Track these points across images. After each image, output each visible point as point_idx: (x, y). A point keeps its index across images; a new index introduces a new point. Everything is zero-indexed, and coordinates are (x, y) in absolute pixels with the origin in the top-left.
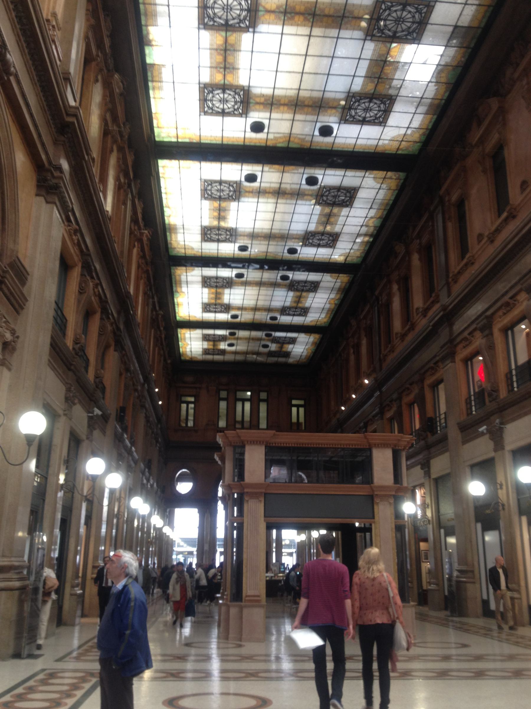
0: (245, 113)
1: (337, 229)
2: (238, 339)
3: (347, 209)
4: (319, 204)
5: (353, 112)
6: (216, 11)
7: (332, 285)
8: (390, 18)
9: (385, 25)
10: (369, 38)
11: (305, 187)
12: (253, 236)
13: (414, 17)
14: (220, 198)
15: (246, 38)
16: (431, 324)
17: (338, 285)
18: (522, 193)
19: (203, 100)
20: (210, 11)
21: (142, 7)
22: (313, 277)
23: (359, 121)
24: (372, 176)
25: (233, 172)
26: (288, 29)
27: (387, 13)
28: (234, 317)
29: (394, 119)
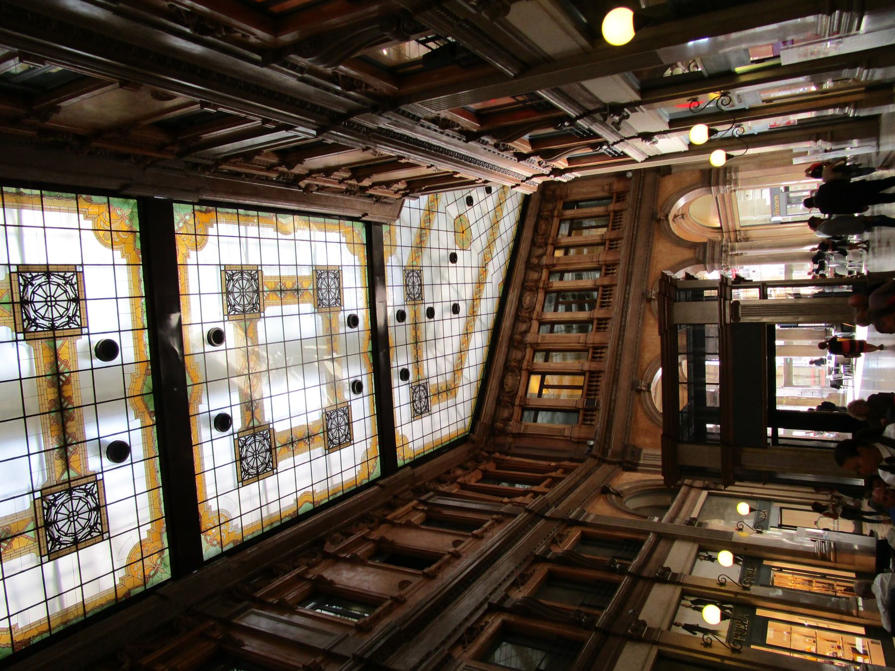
6: (259, 463)
10: (262, 314)
11: (408, 320)
15: (279, 428)
19: (340, 446)
25: (401, 394)
27: (237, 307)
29: (334, 261)
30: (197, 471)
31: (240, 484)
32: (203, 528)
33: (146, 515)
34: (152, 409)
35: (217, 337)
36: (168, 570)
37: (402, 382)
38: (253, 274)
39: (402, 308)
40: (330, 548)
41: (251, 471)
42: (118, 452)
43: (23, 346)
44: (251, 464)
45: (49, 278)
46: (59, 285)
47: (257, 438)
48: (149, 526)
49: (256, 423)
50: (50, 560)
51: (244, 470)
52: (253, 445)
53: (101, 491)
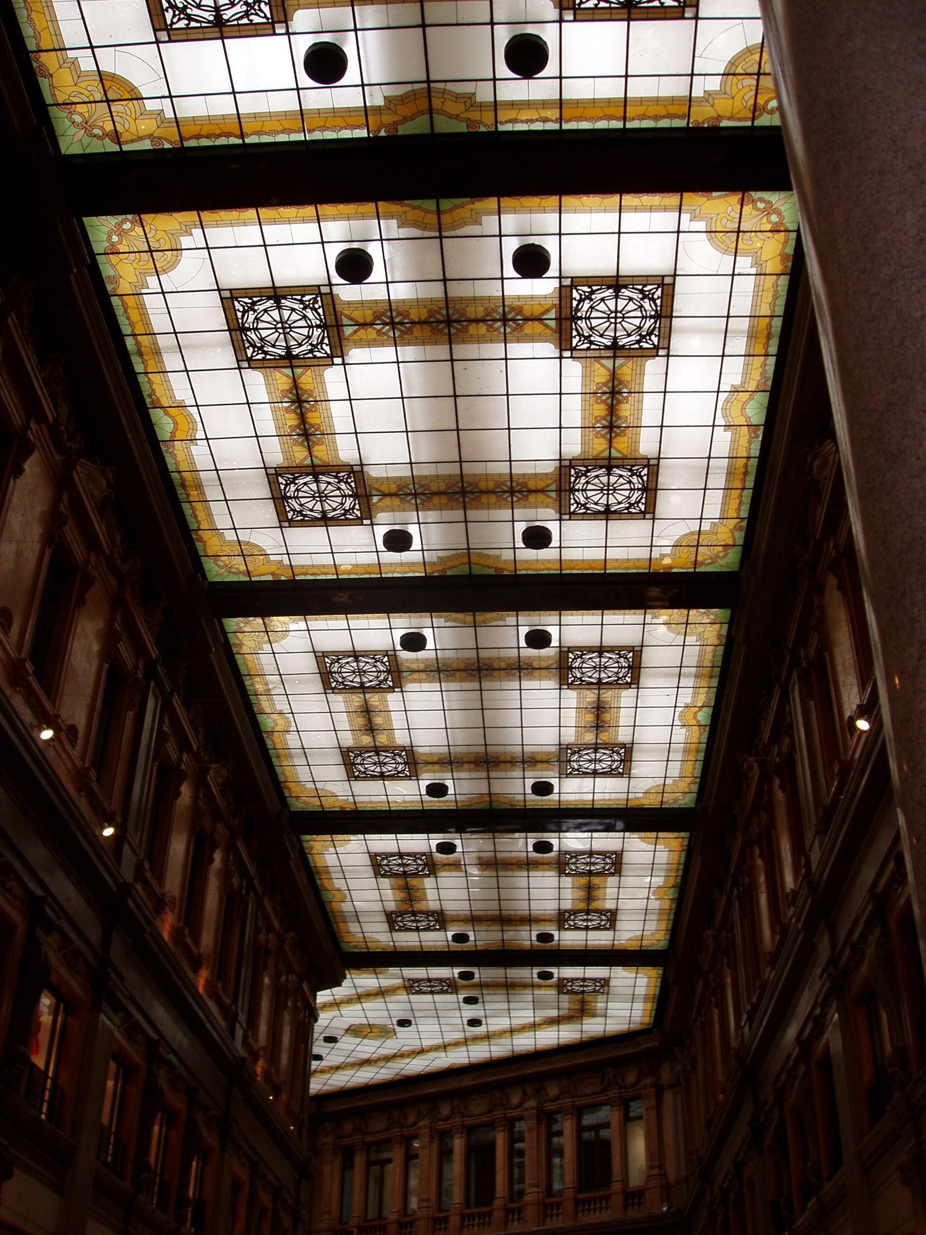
0: (366, 516)
2: (481, 986)
6: (264, 333)
8: (594, 314)
12: (450, 762)
14: (363, 688)
15: (333, 377)
19: (279, 499)
20: (252, 335)
21: (130, 343)
23: (599, 512)
28: (460, 938)
30: (263, 211)
31: (227, 294)
32: (147, 218)
33: (191, 109)
35: (531, 261)
36: (76, 150)
37: (398, 634)
39: (555, 643)
40: (81, 473)
41: (251, 316)
44: (266, 317)
47: (317, 332)
48: (169, 114)
49: (348, 331)
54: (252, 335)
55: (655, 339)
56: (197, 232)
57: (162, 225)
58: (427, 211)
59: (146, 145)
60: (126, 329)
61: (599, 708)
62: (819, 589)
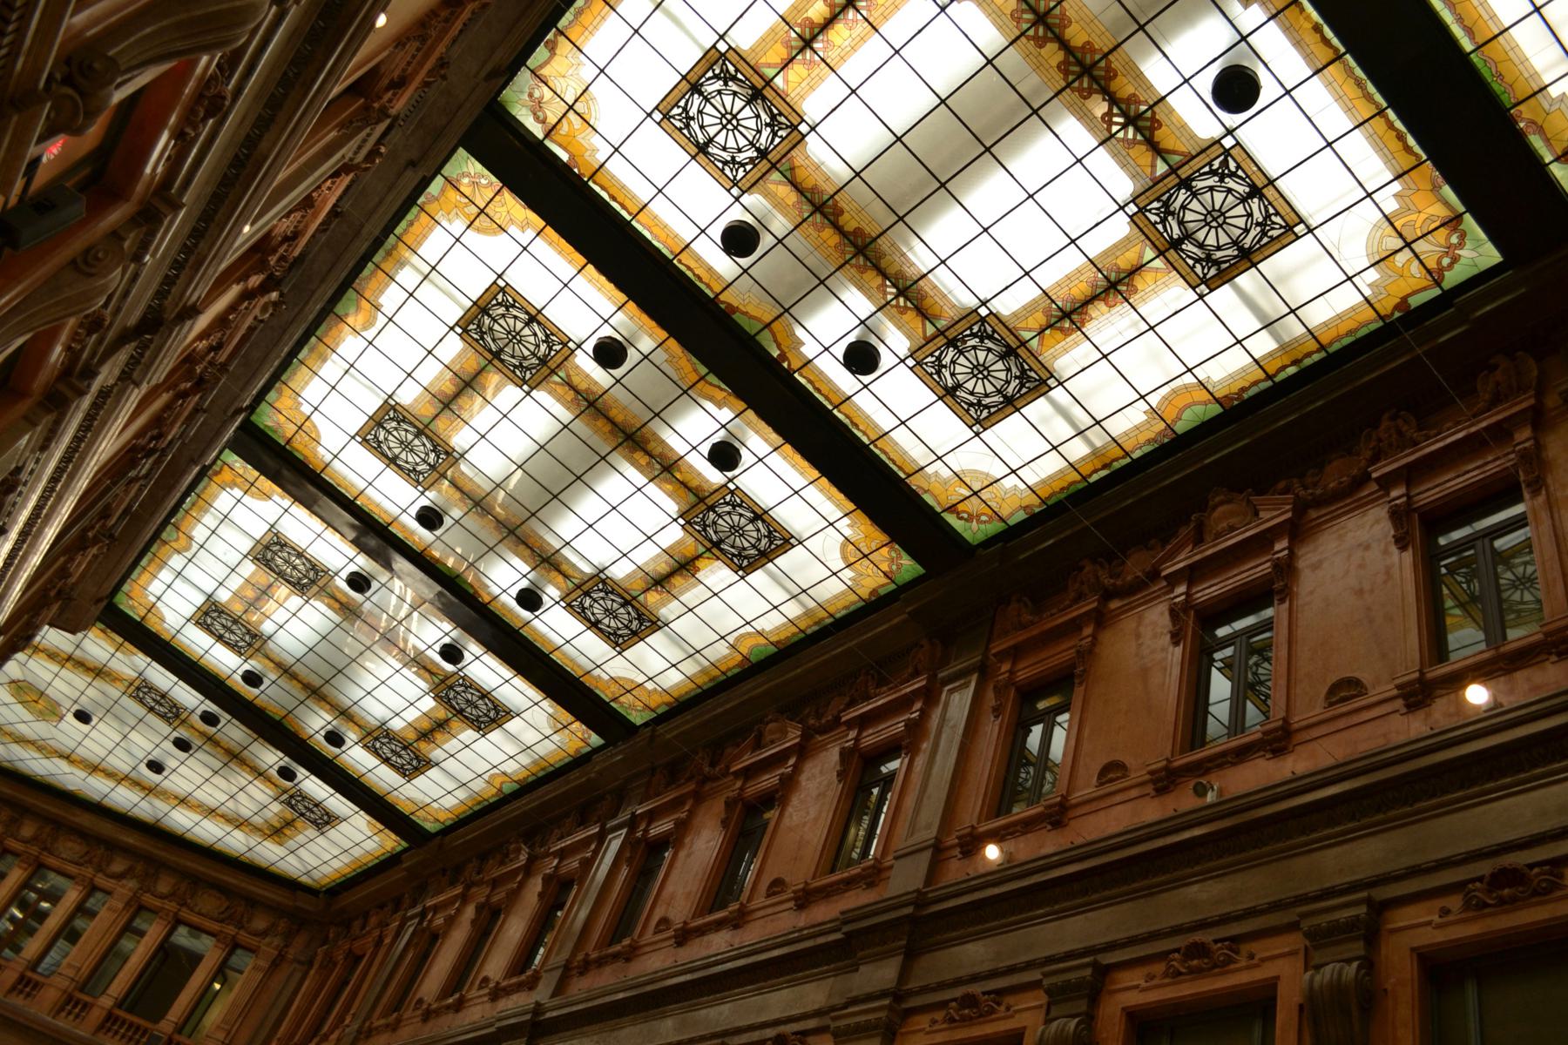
1: (437, 754)
3: (477, 735)
4: (437, 697)
5: (588, 602)
6: (496, 327)
7: (359, 837)
8: (727, 518)
9: (714, 523)
10: (681, 521)
13: (759, 540)
16: (498, 1025)
17: (370, 845)
18: (768, 896)
19: (377, 421)
20: (487, 321)
21: (392, 239)
22: (338, 804)
24: (551, 711)
26: (578, 426)
27: (728, 508)
34: (736, 317)
37: (352, 568)
38: (746, 563)
41: (502, 310)
42: (739, 240)
43: (974, 302)
44: (511, 321)
45: (1005, 396)
46: (987, 395)
47: (535, 361)
48: (601, 158)
50: (714, 46)
51: (513, 306)
52: (532, 348)
53: (717, 174)
54: (487, 321)
55: (745, 563)
56: (531, 234)
57: (511, 207)
58: (695, 370)
59: (564, 157)
60: (398, 231)
61: (441, 725)
62: (699, 798)
